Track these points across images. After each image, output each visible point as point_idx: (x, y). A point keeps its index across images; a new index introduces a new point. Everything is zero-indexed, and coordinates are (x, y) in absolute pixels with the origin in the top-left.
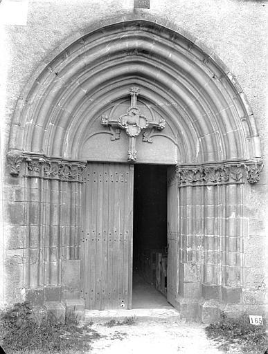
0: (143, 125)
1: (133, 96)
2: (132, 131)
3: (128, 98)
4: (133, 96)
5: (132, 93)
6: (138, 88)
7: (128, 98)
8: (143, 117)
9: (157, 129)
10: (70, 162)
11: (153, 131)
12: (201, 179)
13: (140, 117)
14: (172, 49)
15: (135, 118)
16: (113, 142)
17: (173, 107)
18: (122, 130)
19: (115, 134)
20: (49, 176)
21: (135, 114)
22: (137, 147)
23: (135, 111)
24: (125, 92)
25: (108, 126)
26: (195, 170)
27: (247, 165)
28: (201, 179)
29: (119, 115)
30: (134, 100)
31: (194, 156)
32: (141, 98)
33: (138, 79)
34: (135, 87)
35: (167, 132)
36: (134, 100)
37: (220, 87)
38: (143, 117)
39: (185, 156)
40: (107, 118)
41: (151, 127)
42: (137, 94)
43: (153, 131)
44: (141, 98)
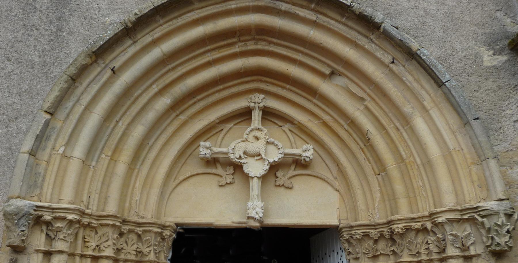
0: (274, 156)
1: (253, 109)
2: (255, 169)
3: (245, 114)
4: (253, 109)
5: (252, 105)
6: (262, 96)
7: (245, 114)
8: (273, 143)
9: (300, 164)
10: (139, 225)
11: (293, 167)
12: (388, 251)
13: (268, 143)
14: (314, 24)
15: (257, 146)
16: (222, 189)
17: (325, 124)
18: (237, 168)
19: (227, 175)
20: (94, 250)
21: (257, 138)
22: (263, 197)
23: (257, 133)
24: (241, 103)
25: (212, 162)
26: (373, 232)
27: (483, 217)
28: (388, 251)
29: (235, 144)
30: (257, 115)
31: (371, 211)
32: (268, 114)
33: (261, 81)
34: (257, 95)
35: (320, 169)
36: (257, 115)
37: (408, 78)
38: (273, 143)
39: (355, 208)
40: (205, 148)
41: (290, 160)
42: (261, 105)
43: (293, 167)
44: (268, 114)
